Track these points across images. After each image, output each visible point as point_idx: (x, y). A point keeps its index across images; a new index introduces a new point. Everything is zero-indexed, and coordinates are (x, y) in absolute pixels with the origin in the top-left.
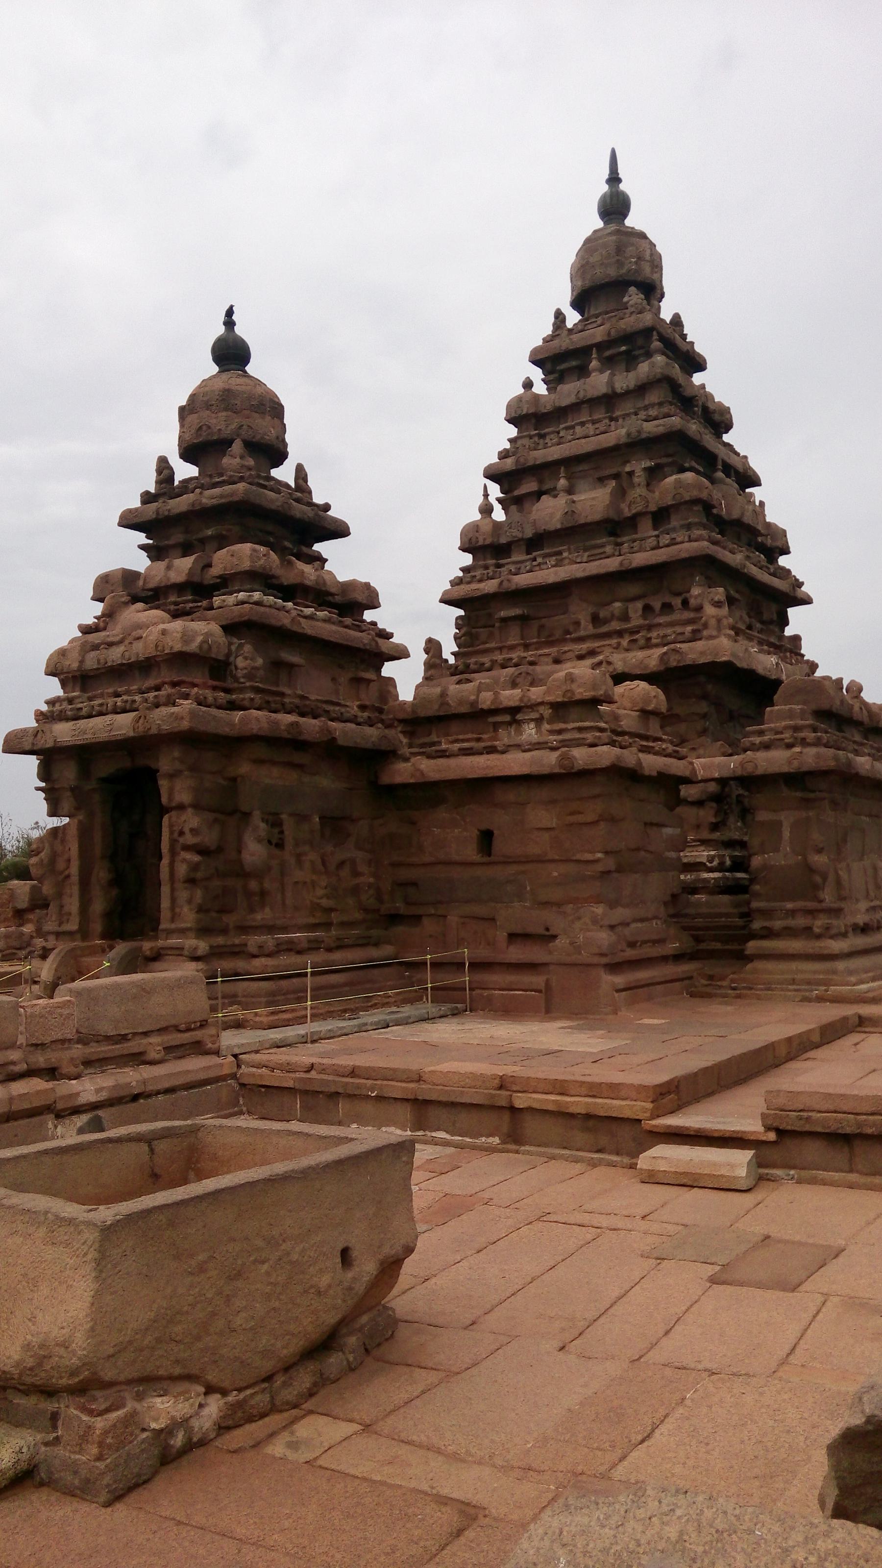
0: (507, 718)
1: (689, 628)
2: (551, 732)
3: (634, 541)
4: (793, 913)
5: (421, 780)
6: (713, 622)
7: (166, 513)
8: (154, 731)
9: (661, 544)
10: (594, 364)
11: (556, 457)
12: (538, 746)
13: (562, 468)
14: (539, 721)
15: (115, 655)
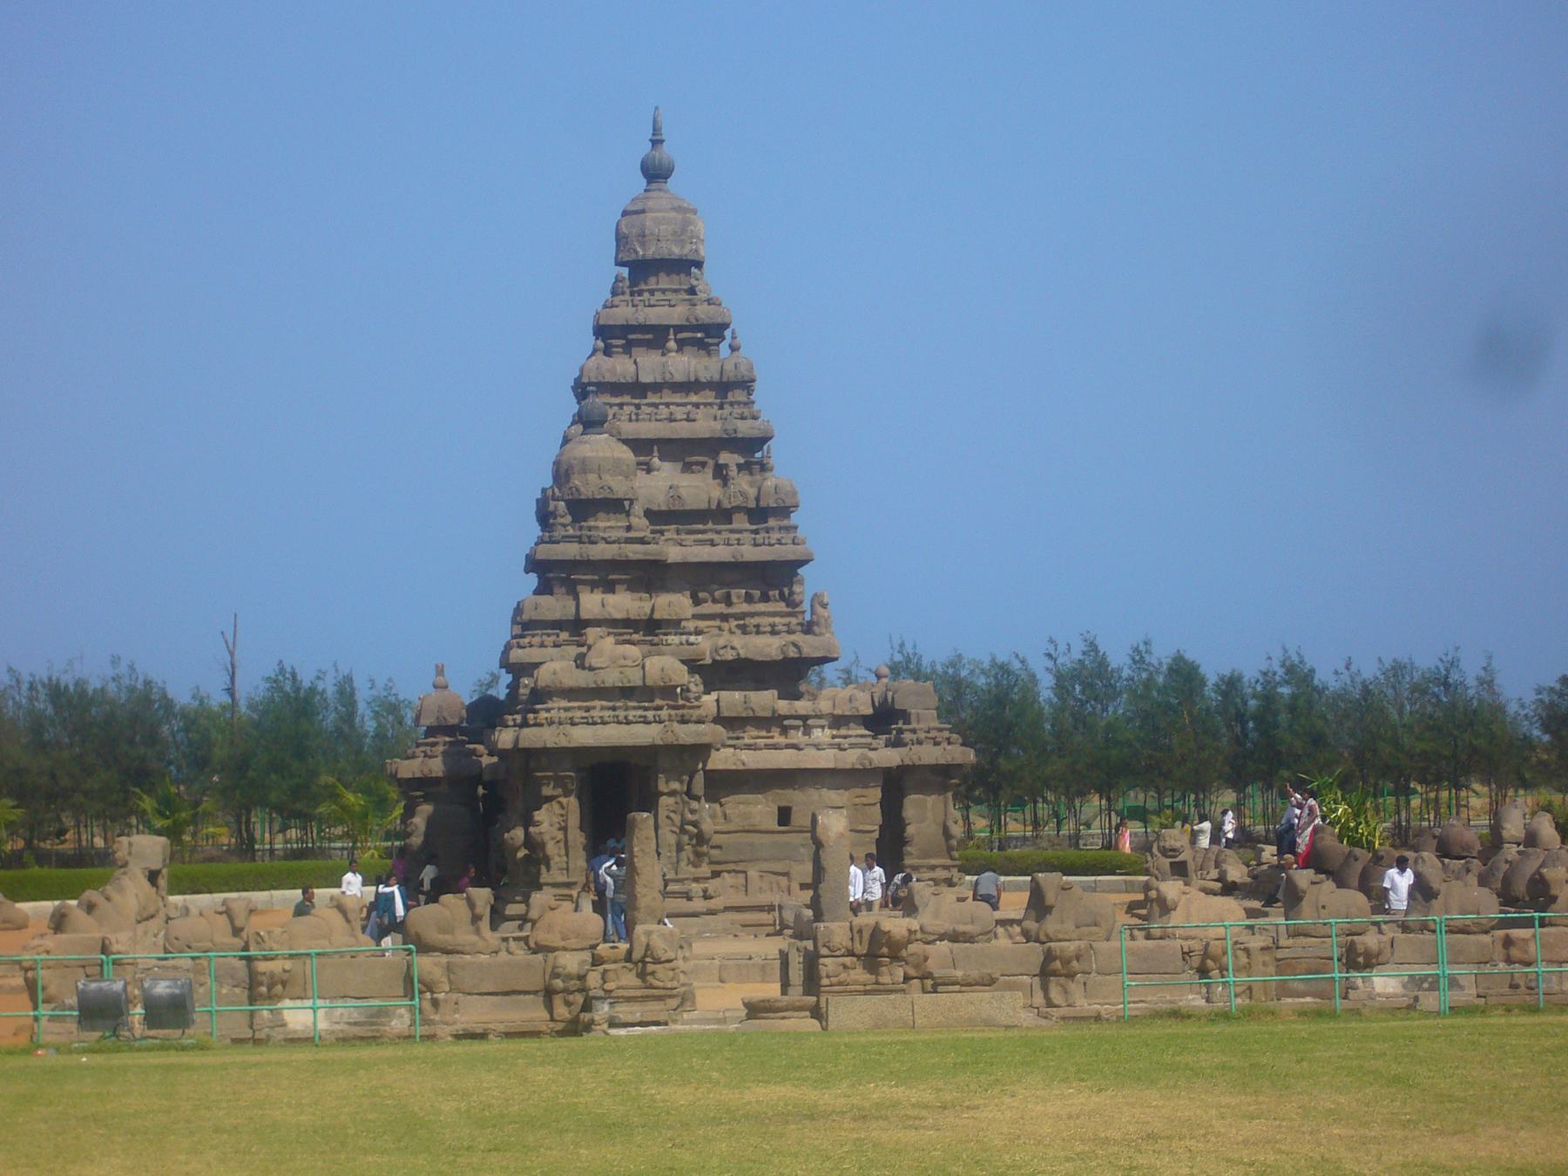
0: (799, 723)
1: (794, 621)
2: (834, 737)
3: (732, 531)
4: (933, 868)
5: (741, 767)
6: (823, 620)
7: (591, 558)
8: (681, 742)
9: (767, 542)
10: (672, 344)
11: (650, 436)
12: (832, 746)
13: (655, 448)
14: (823, 727)
15: (611, 678)
